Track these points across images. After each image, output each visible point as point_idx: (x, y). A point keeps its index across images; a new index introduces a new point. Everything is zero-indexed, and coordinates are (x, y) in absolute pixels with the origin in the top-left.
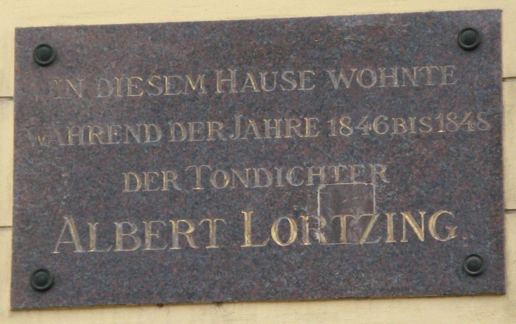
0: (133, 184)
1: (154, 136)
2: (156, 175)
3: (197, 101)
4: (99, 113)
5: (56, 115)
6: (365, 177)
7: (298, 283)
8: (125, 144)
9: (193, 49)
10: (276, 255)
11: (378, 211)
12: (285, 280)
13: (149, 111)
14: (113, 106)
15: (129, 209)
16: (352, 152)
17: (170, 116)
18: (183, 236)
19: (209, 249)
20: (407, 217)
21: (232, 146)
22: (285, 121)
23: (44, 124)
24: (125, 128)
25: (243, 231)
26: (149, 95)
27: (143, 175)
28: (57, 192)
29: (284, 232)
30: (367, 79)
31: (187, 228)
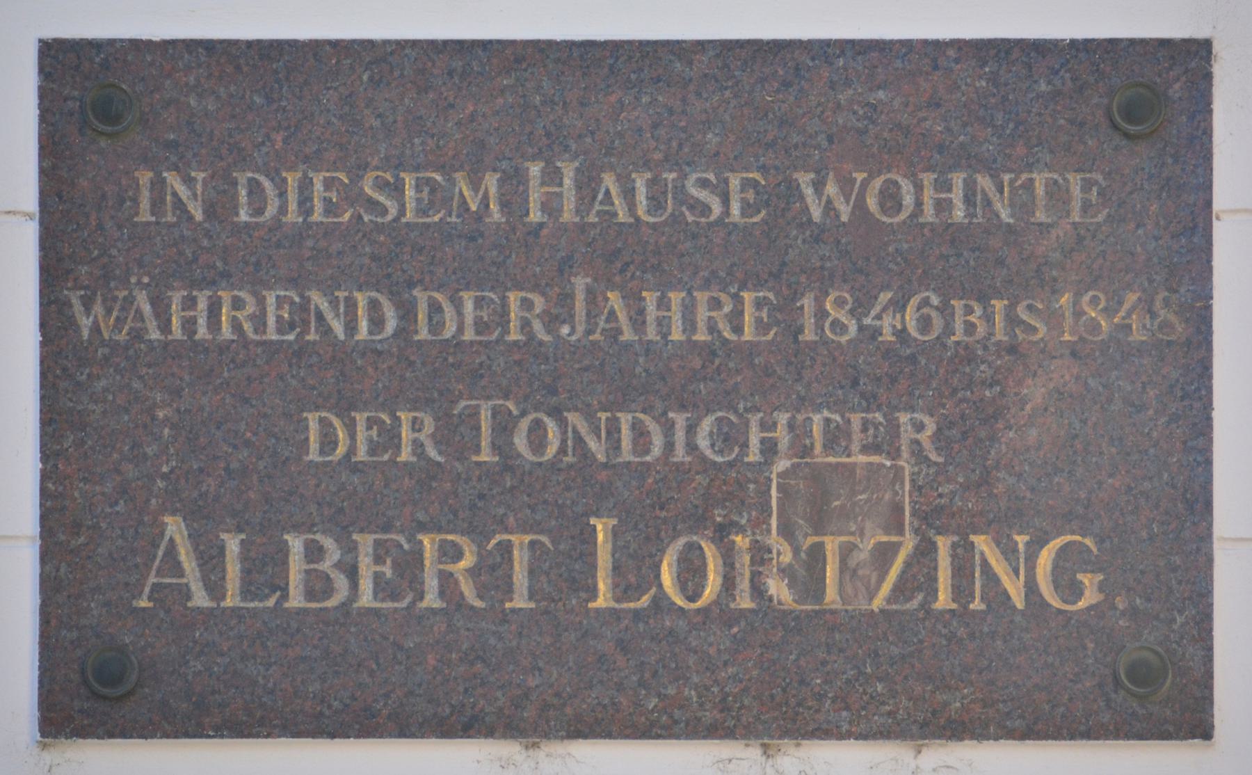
0: (328, 443)
1: (377, 323)
2: (384, 422)
3: (480, 241)
4: (246, 263)
5: (141, 264)
6: (885, 443)
7: (724, 699)
8: (308, 341)
9: (472, 108)
10: (671, 632)
11: (916, 531)
12: (693, 693)
13: (367, 261)
14: (279, 245)
15: (319, 504)
16: (855, 383)
17: (417, 277)
18: (451, 574)
19: (513, 610)
20: (982, 543)
21: (567, 356)
22: (693, 299)
23: (112, 284)
24: (309, 300)
25: (594, 567)
26: (366, 219)
27: (354, 420)
28: (145, 454)
29: (691, 572)
30: (890, 198)
31: (459, 556)
